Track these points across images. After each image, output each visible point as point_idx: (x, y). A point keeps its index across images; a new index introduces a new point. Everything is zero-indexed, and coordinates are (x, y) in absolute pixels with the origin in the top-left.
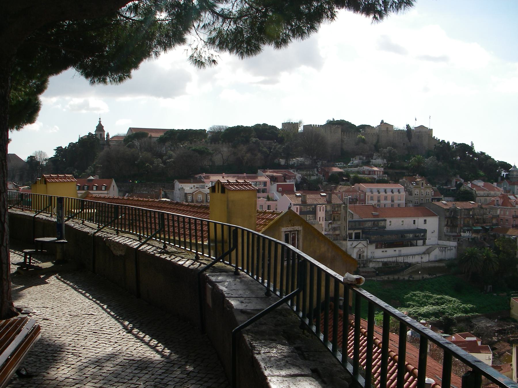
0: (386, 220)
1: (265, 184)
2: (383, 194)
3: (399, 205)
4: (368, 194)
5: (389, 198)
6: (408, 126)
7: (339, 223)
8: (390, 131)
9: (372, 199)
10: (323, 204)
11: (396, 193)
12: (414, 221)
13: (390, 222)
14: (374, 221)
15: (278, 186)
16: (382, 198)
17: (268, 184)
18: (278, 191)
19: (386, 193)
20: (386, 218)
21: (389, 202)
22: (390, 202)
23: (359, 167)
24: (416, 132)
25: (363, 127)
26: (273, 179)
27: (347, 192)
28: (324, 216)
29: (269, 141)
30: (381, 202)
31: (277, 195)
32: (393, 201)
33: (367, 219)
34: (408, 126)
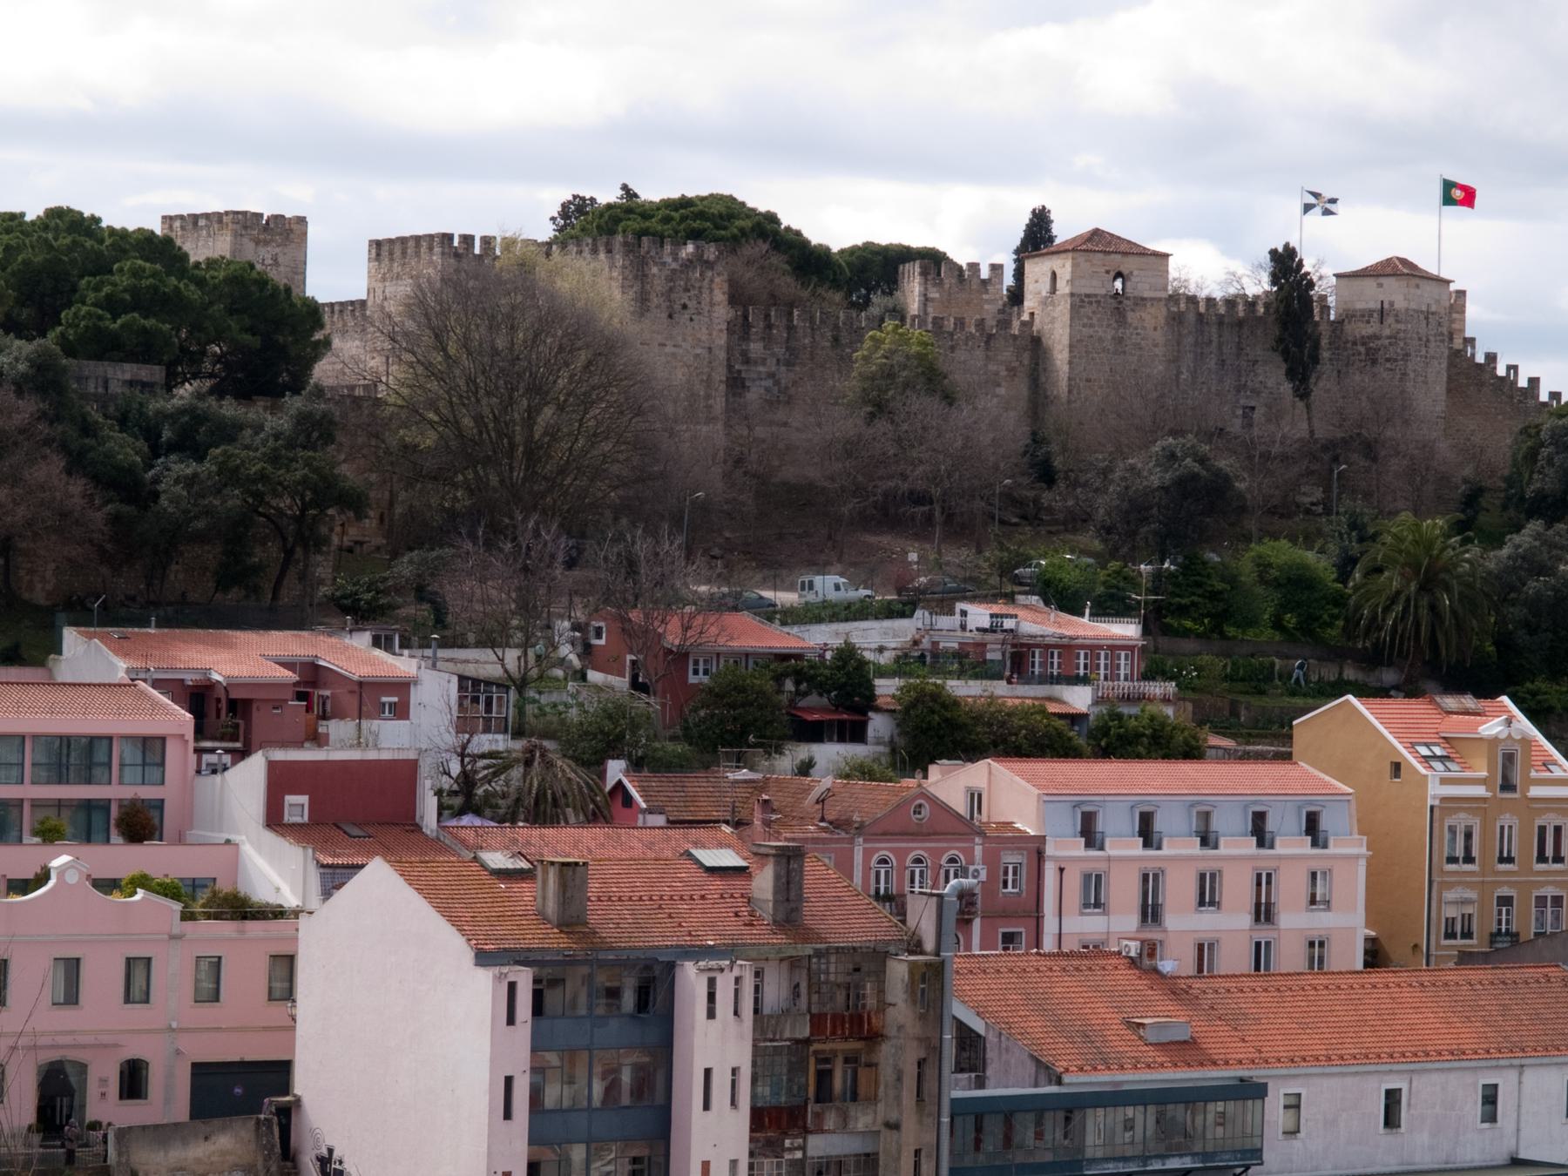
0: (1257, 1091)
1: (151, 748)
2: (1179, 847)
3: (1317, 947)
4: (1065, 848)
5: (1237, 890)
6: (1285, 263)
7: (863, 1120)
8: (1141, 302)
9: (1094, 896)
10: (730, 951)
11: (1179, 847)
12: (1490, 1097)
13: (1294, 1104)
14: (1159, 1098)
15: (280, 781)
16: (1178, 891)
17: (179, 758)
18: (274, 819)
19: (1207, 840)
20: (1256, 1074)
21: (1232, 923)
22: (1245, 920)
23: (921, 617)
24: (1348, 316)
25: (879, 267)
26: (223, 718)
27: (886, 835)
28: (742, 1055)
29: (128, 371)
30: (1171, 921)
31: (274, 870)
32: (1264, 912)
33: (1103, 1079)
34: (1285, 263)
